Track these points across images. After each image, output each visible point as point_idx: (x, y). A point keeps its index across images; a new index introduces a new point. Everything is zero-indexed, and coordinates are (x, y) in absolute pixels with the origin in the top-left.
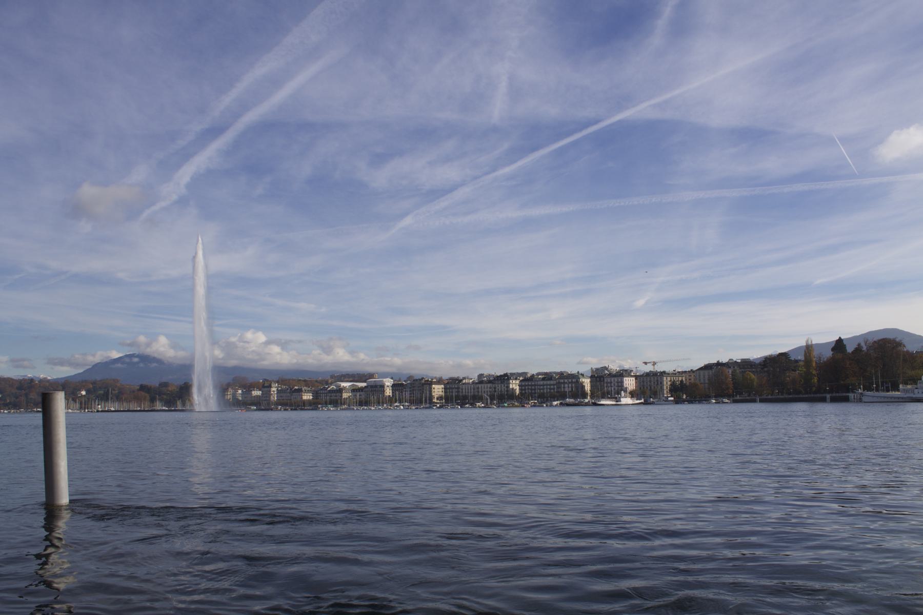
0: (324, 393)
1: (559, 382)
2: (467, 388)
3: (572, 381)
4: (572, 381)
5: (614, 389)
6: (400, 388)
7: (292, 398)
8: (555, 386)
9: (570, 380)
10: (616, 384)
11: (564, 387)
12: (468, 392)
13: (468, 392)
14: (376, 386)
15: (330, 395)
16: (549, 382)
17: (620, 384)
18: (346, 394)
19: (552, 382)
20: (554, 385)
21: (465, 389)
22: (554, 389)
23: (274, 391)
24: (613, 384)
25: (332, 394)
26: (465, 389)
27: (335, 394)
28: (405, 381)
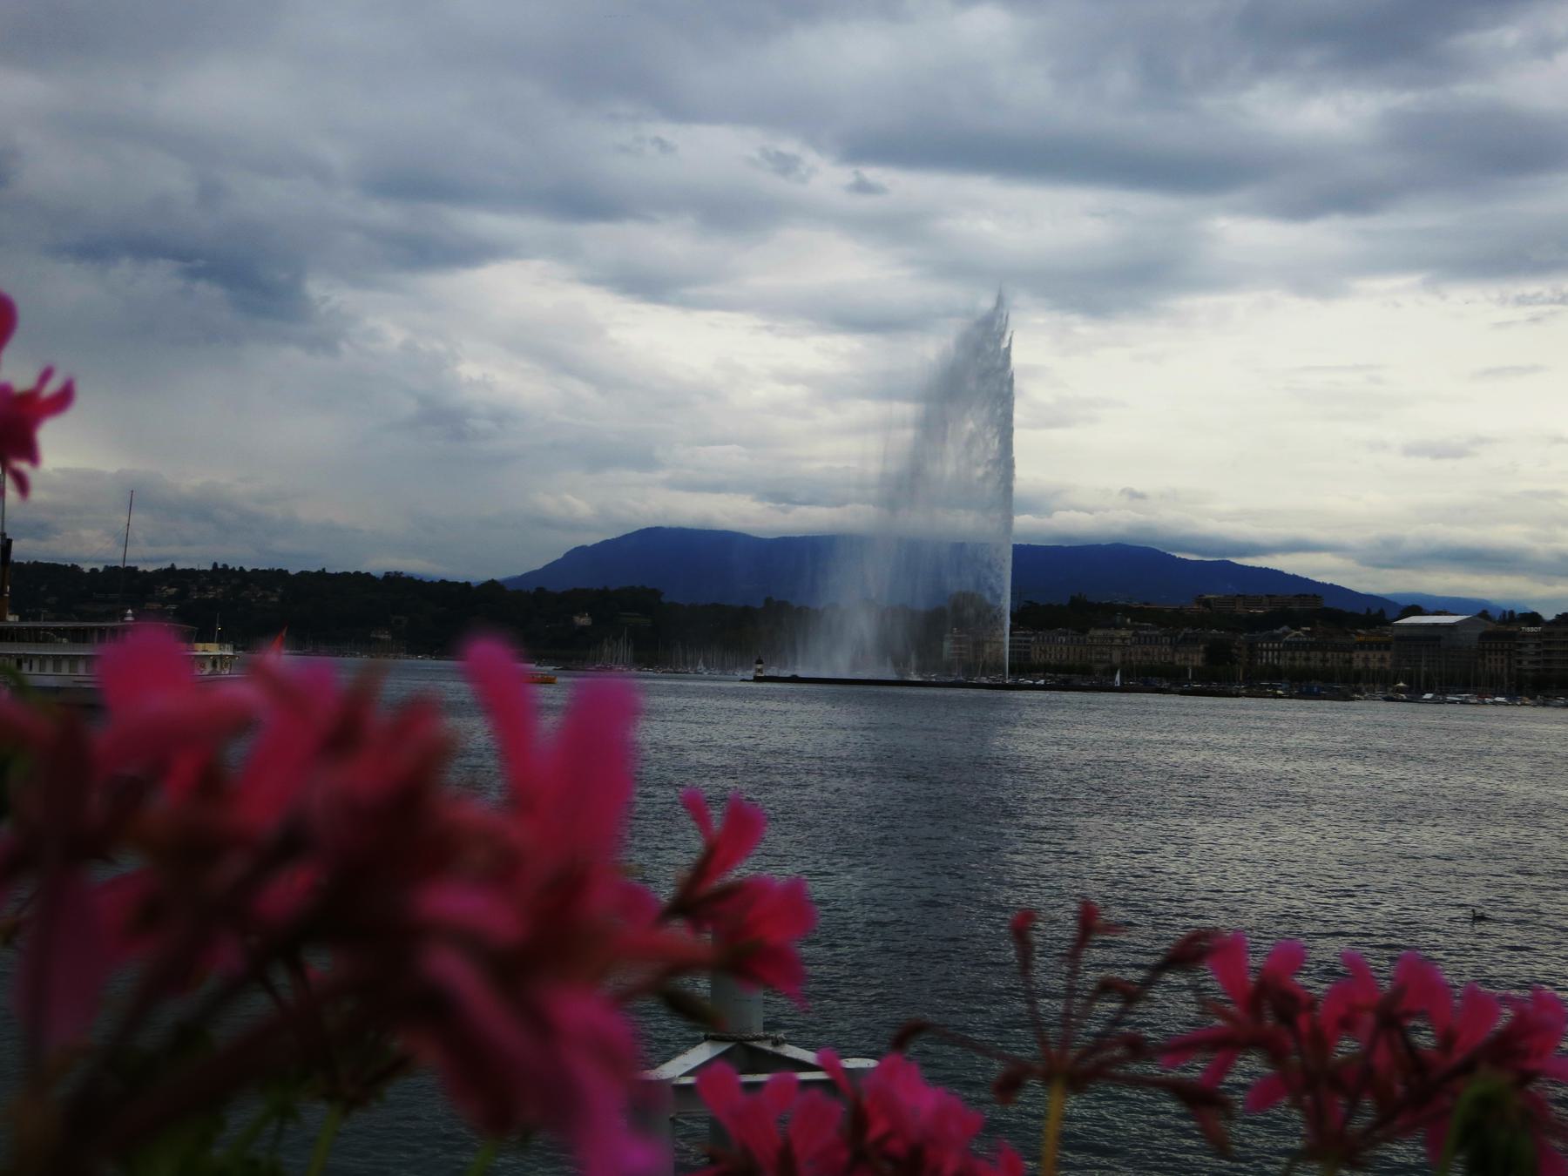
0: (1273, 650)
7: (1177, 658)
15: (1289, 654)
18: (1335, 654)
23: (1123, 639)
27: (1304, 654)
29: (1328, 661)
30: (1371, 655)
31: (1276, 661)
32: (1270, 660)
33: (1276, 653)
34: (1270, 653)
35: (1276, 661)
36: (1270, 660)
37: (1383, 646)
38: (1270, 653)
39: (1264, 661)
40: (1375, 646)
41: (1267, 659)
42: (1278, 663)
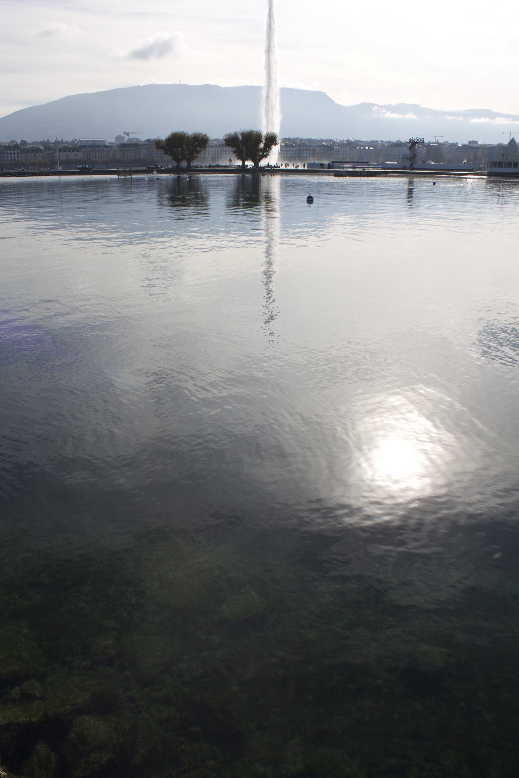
1: (300, 149)
2: (214, 150)
3: (304, 148)
4: (304, 148)
5: (341, 156)
6: (134, 149)
8: (297, 152)
9: (308, 148)
10: (340, 153)
11: (304, 153)
12: (215, 154)
13: (215, 154)
14: (98, 146)
15: (24, 155)
16: (291, 149)
17: (345, 153)
19: (294, 149)
20: (295, 151)
21: (212, 151)
22: (295, 154)
24: (342, 153)
25: (29, 155)
26: (212, 151)
27: (33, 155)
28: (108, 143)
29: (37, 157)
30: (69, 154)
31: (16, 158)
32: (13, 158)
33: (16, 155)
34: (13, 155)
35: (16, 158)
36: (13, 158)
37: (71, 150)
38: (13, 155)
39: (9, 158)
40: (75, 150)
41: (11, 157)
42: (18, 158)
